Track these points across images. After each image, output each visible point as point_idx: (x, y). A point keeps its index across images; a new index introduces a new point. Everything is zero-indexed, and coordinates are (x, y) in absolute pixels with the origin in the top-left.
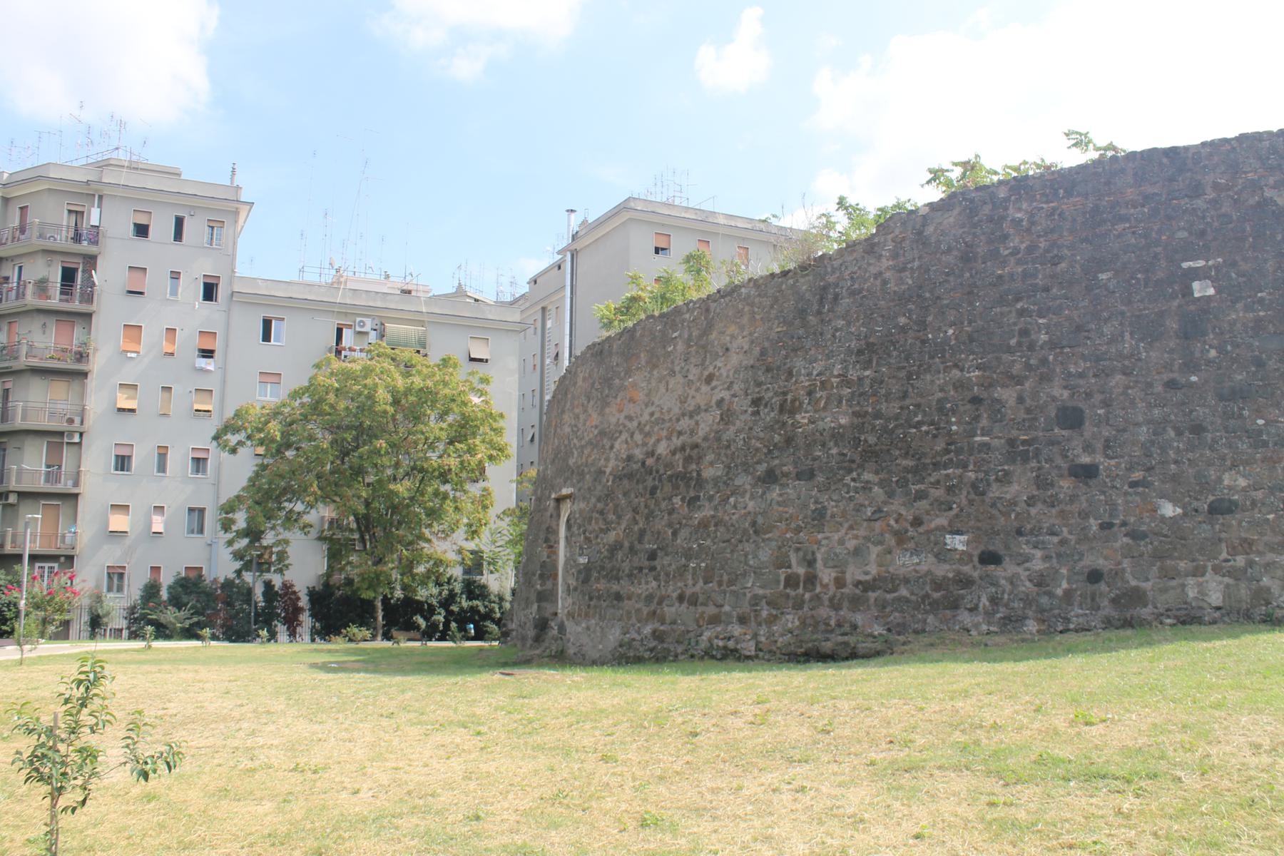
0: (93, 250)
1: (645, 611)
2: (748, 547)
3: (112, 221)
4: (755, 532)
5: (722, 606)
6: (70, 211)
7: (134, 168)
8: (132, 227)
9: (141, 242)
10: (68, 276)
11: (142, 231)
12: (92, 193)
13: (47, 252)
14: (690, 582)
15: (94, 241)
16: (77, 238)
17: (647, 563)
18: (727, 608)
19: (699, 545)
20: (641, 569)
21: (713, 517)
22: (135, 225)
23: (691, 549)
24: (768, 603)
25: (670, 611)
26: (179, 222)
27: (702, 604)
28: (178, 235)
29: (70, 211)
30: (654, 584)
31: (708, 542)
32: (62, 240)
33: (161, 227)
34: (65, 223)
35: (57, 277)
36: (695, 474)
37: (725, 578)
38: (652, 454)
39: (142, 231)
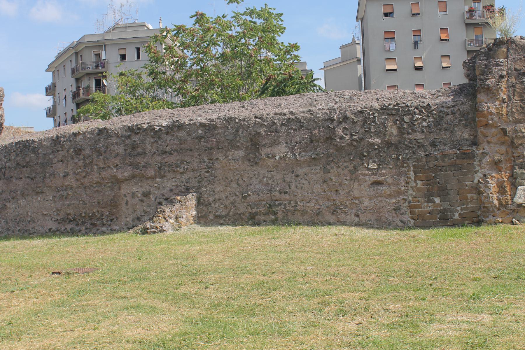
0: (103, 70)
3: (109, 55)
6: (96, 55)
7: (126, 27)
8: (119, 57)
9: (123, 63)
10: (98, 83)
11: (123, 57)
12: (100, 45)
13: (88, 74)
15: (103, 67)
16: (97, 67)
22: (121, 55)
26: (138, 50)
28: (138, 57)
29: (96, 55)
32: (92, 69)
33: (131, 54)
34: (93, 60)
35: (93, 84)
39: (123, 57)
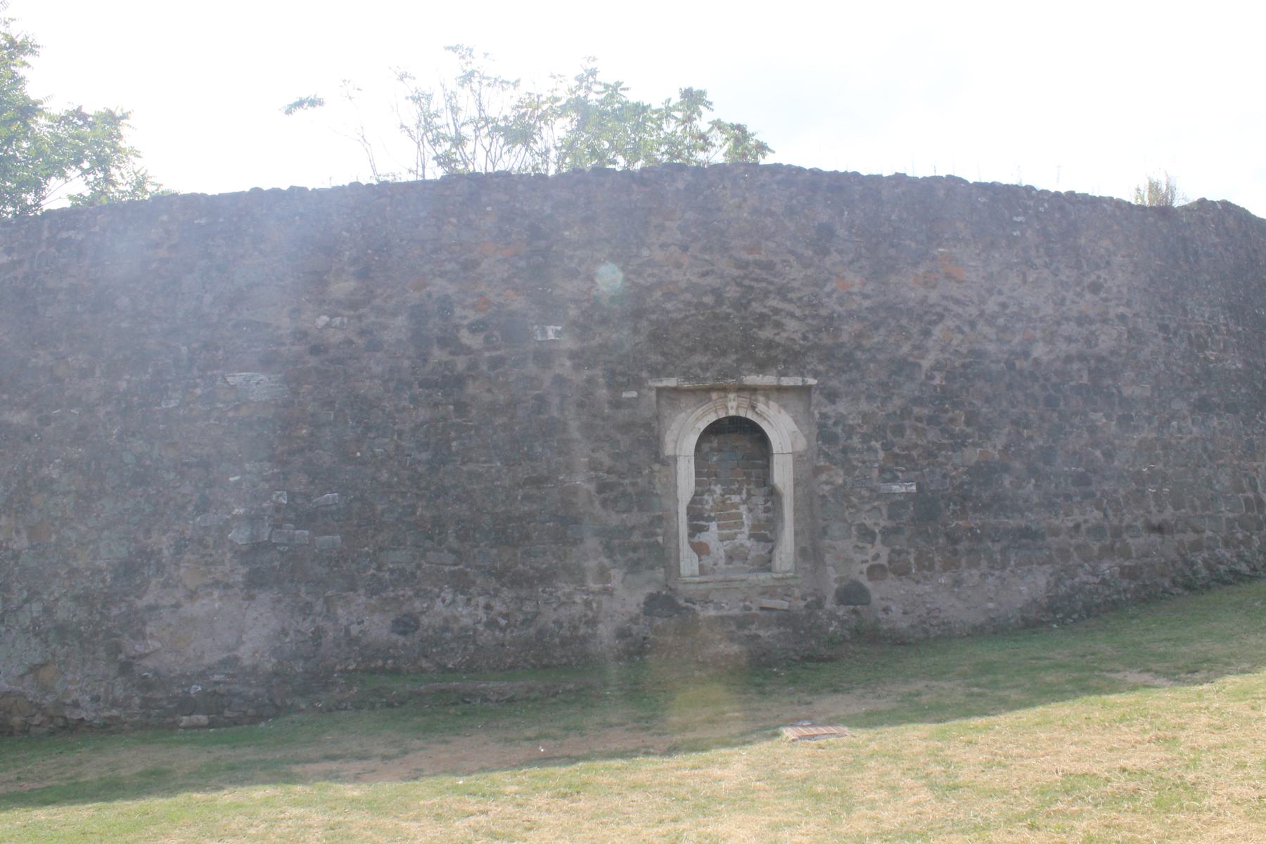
1: (1096, 547)
2: (1205, 472)
4: (1210, 457)
5: (1203, 531)
14: (1154, 510)
17: (1073, 489)
18: (1209, 533)
19: (1150, 469)
20: (1068, 497)
21: (1157, 439)
23: (1139, 472)
24: (1241, 526)
25: (1137, 543)
27: (1178, 532)
30: (1098, 514)
31: (1160, 466)
36: (1114, 390)
37: (1197, 503)
38: (1026, 354)
